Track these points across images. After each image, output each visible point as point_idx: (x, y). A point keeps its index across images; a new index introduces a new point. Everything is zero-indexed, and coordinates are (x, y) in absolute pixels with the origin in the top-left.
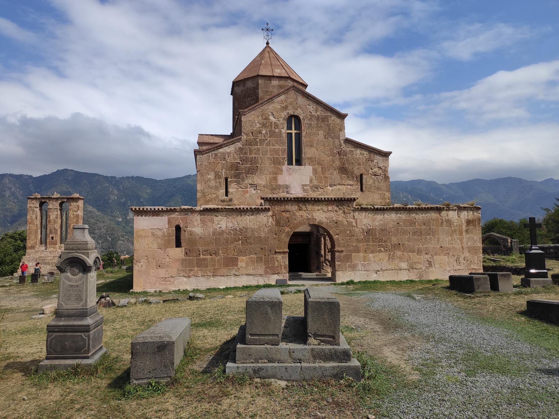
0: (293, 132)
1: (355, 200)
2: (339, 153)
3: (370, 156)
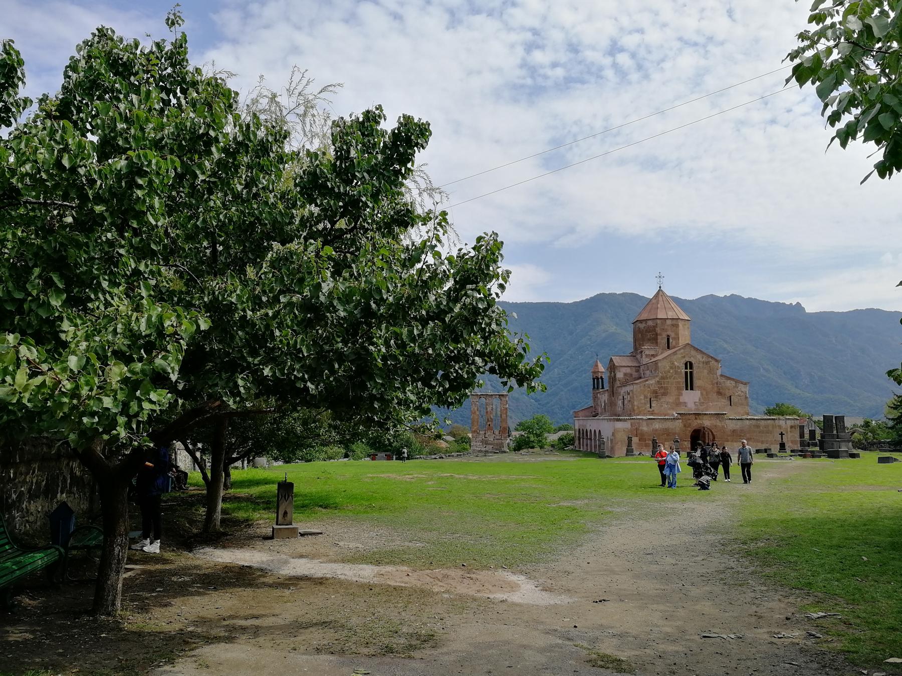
0: (689, 370)
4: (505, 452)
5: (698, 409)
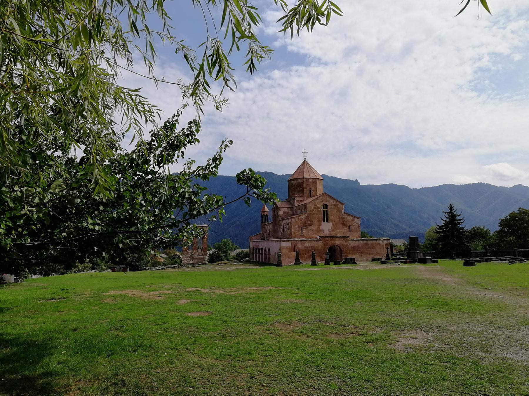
0: (325, 210)
1: (349, 237)
4: (206, 264)
5: (331, 234)
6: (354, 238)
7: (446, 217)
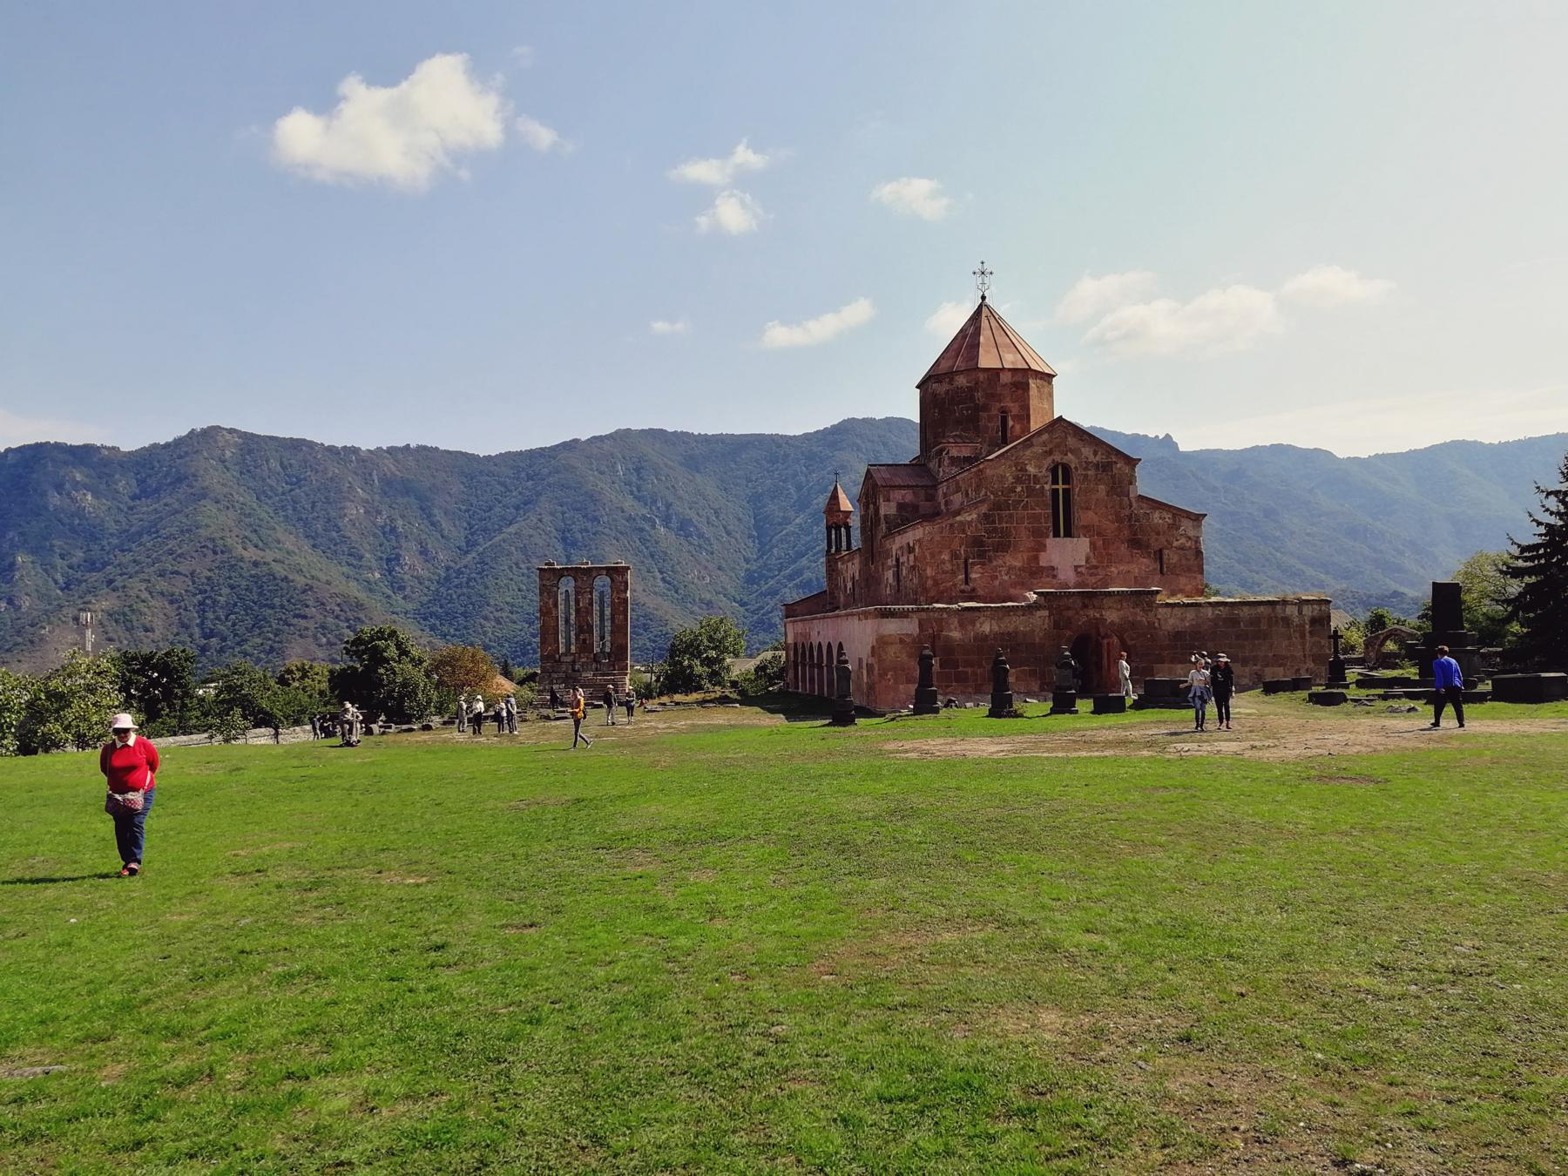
0: (1060, 487)
1: (1158, 592)
2: (1130, 517)
3: (1175, 521)
6: (1179, 596)
7: (1547, 510)
